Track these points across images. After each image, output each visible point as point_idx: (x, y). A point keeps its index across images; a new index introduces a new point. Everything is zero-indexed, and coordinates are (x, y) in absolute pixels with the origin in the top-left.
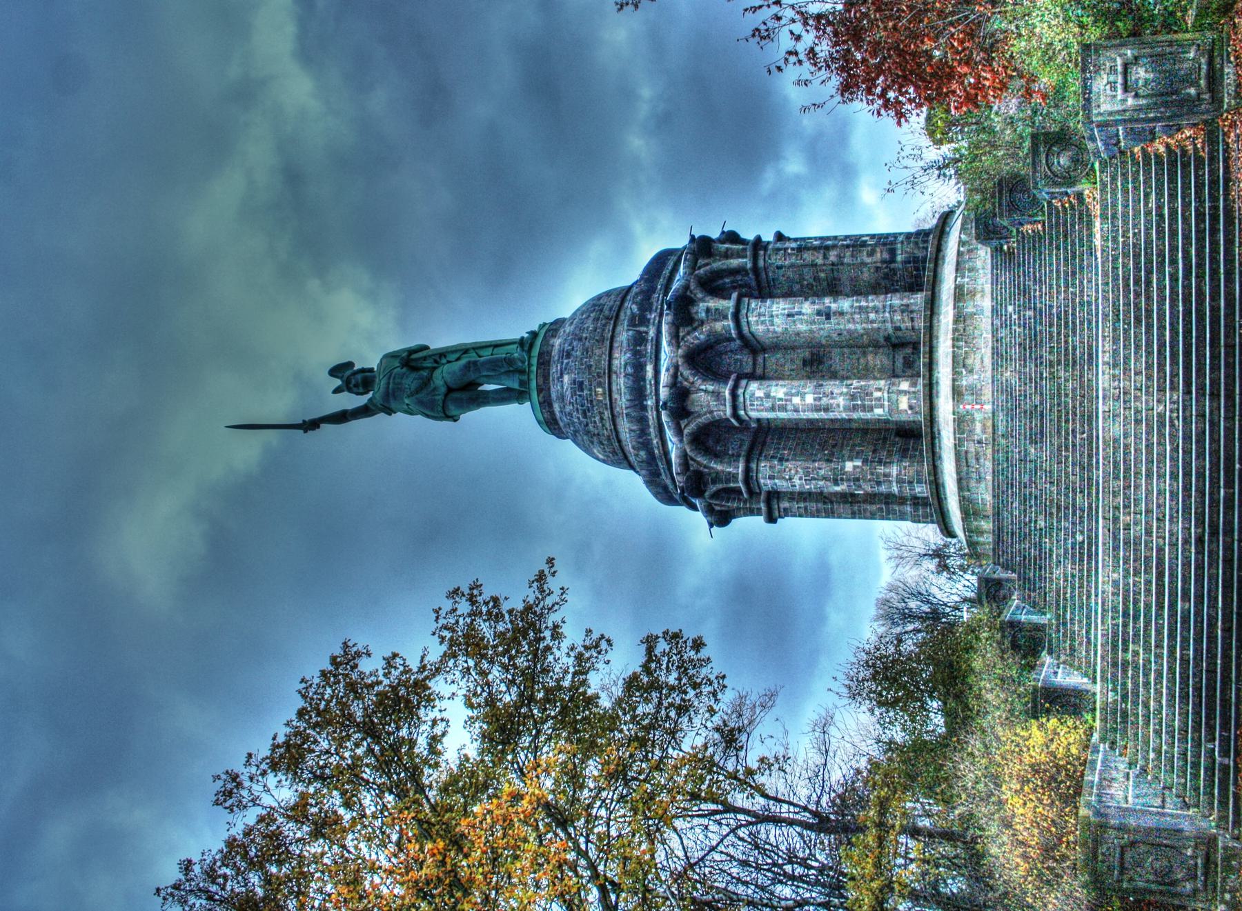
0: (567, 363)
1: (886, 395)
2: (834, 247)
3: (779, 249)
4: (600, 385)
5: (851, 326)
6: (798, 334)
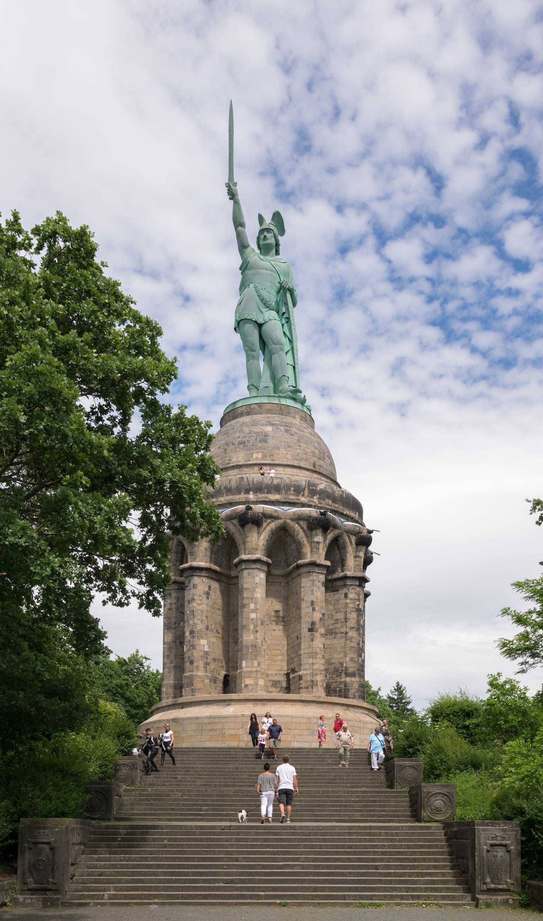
0: (281, 430)
1: (254, 669)
2: (359, 634)
3: (359, 595)
4: (264, 457)
5: (303, 646)
6: (299, 608)
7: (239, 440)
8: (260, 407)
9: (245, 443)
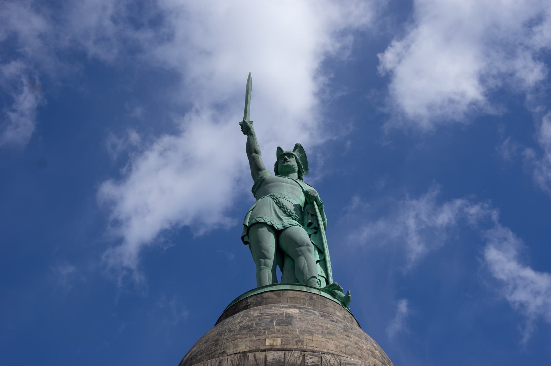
0: (314, 314)
7: (241, 325)
8: (279, 295)
9: (252, 327)
